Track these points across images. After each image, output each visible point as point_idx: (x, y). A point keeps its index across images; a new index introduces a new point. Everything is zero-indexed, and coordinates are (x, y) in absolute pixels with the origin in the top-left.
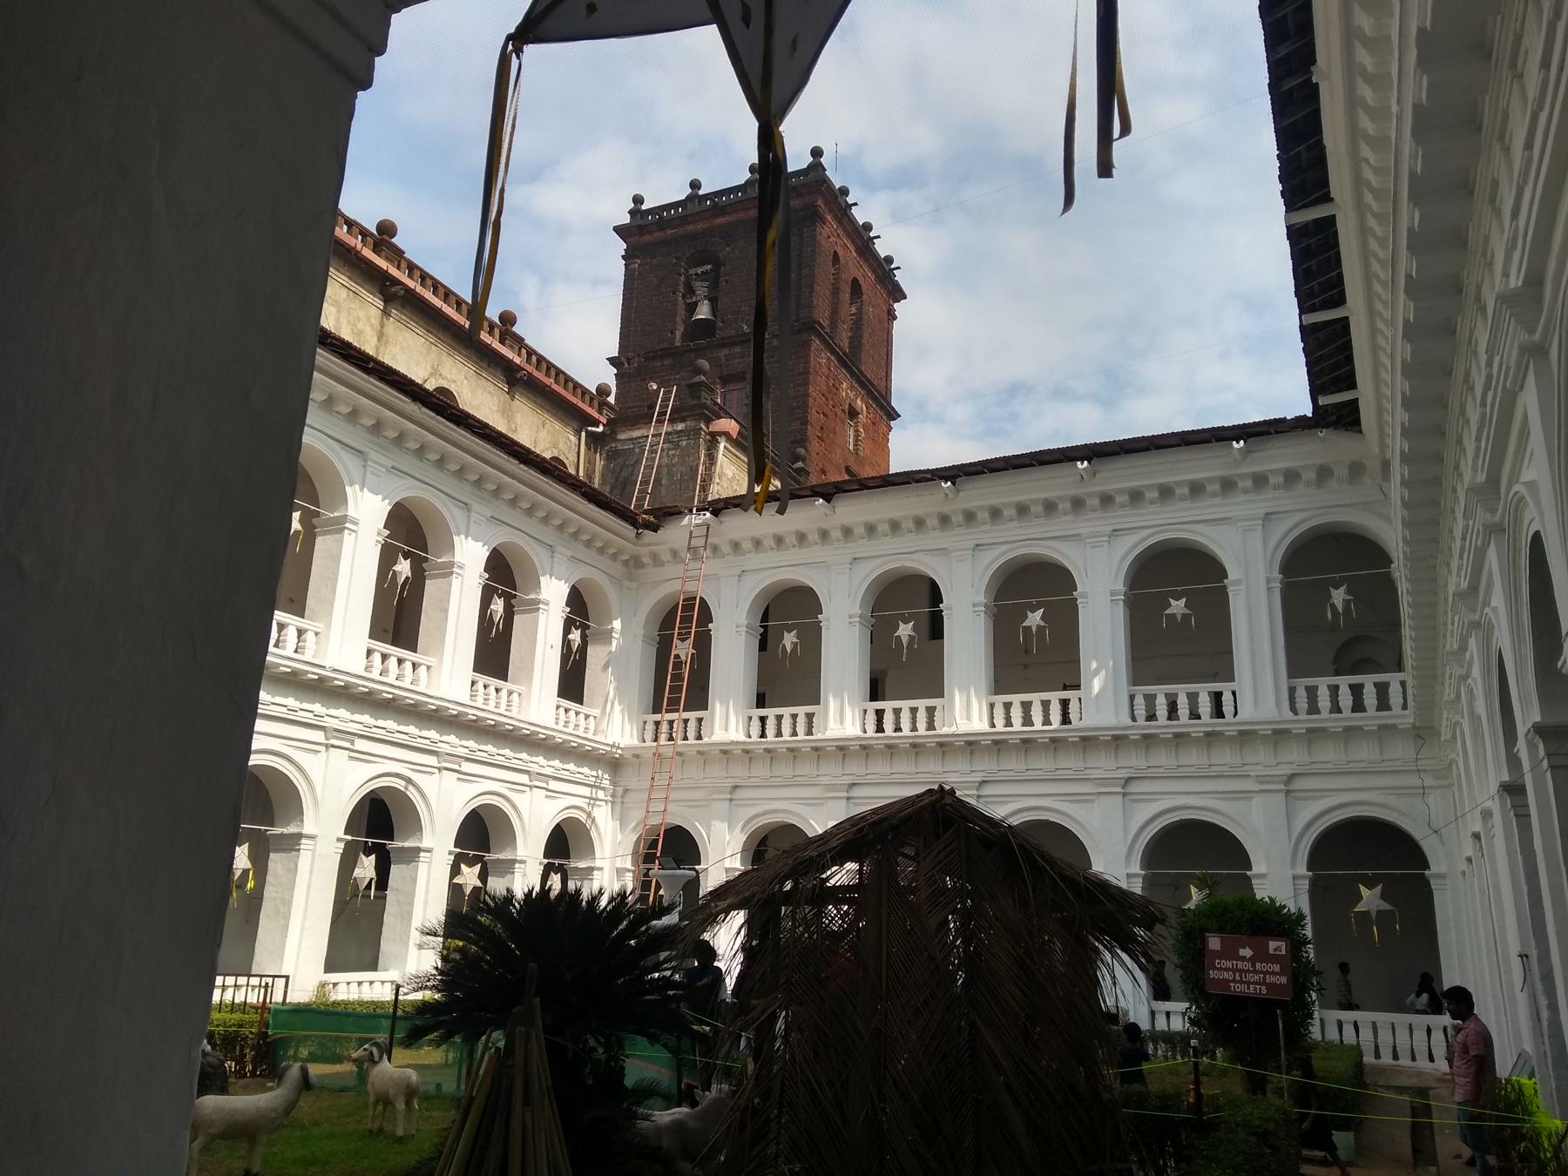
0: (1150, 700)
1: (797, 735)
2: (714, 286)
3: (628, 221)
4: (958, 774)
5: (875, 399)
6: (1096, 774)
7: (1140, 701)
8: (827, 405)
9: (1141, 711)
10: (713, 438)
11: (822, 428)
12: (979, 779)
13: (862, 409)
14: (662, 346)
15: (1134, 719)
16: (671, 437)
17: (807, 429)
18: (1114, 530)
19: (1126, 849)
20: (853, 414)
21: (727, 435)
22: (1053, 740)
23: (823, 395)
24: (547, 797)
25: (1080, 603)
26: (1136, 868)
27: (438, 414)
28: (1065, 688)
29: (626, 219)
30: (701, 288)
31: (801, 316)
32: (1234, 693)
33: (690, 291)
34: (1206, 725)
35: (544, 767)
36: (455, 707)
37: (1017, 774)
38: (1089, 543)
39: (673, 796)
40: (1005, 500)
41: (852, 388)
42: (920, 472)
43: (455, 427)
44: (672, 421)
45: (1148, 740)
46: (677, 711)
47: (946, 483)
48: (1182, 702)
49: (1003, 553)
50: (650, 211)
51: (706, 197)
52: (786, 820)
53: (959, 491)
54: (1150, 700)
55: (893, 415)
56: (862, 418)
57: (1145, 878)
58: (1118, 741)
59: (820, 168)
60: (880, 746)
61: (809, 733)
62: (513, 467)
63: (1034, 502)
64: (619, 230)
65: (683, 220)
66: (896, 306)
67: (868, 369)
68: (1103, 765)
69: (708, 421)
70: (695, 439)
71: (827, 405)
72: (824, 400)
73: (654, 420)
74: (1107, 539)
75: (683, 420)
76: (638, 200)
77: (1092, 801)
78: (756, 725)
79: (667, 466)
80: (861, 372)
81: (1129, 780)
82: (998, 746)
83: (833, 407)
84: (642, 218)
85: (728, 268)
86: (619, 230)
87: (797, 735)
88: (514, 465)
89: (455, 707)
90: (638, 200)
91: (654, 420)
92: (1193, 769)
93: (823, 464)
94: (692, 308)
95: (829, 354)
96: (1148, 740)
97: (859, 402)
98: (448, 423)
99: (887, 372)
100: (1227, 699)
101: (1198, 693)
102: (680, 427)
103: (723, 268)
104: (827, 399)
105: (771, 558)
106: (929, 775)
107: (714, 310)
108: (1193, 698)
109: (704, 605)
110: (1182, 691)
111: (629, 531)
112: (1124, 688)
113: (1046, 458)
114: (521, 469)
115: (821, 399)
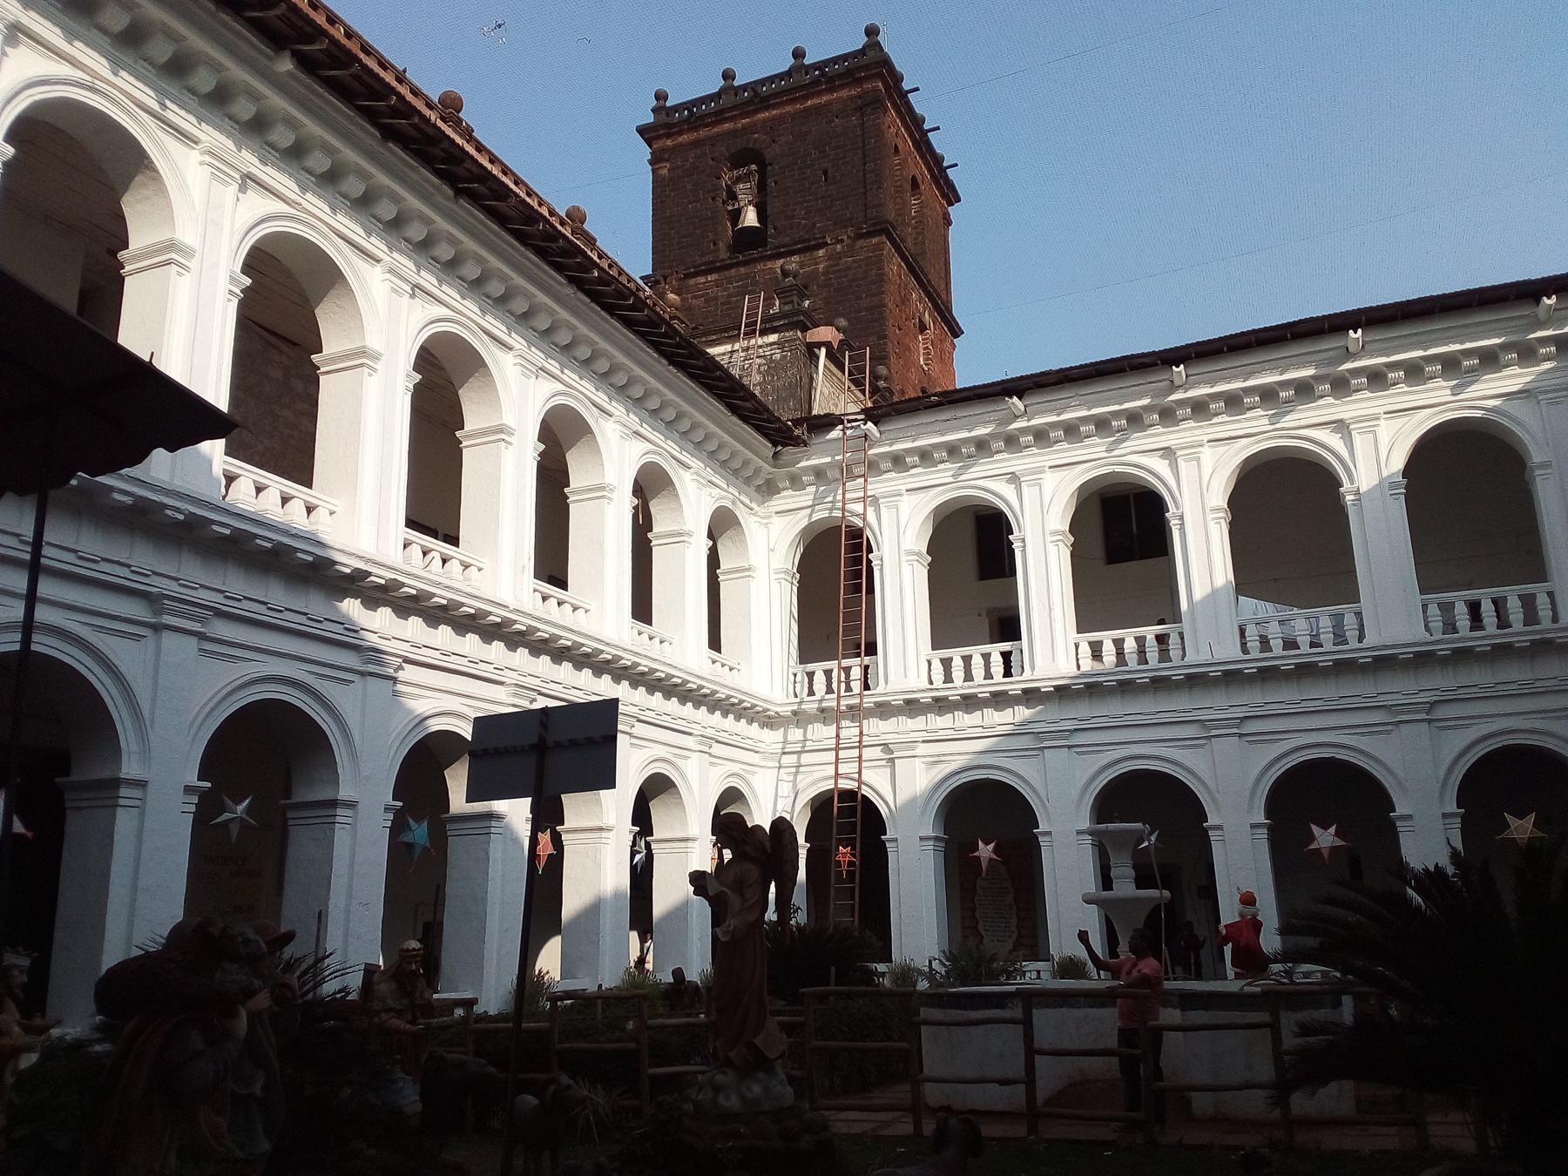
0: (1447, 608)
1: (814, 695)
2: (762, 187)
3: (652, 120)
4: (1211, 711)
6: (1390, 700)
7: (1433, 610)
9: (1436, 624)
12: (1242, 715)
14: (706, 259)
15: (1245, 650)
16: (761, 350)
17: (885, 344)
19: (1440, 785)
20: (923, 328)
21: (828, 345)
22: (1154, 680)
24: (711, 764)
26: (1452, 807)
27: (593, 301)
28: (1161, 622)
29: (650, 118)
30: (744, 191)
31: (869, 216)
32: (1551, 595)
33: (733, 196)
34: (1493, 637)
35: (706, 728)
36: (631, 657)
37: (1325, 703)
39: (867, 753)
42: (1143, 355)
43: (609, 318)
44: (763, 333)
45: (1462, 656)
46: (858, 655)
47: (1178, 367)
48: (1487, 608)
49: (1247, 447)
50: (676, 108)
51: (744, 88)
52: (990, 777)
54: (1447, 608)
57: (1463, 817)
58: (1422, 660)
59: (877, 48)
60: (1145, 680)
61: (1008, 673)
62: (663, 369)
64: (642, 131)
65: (719, 116)
66: (950, 209)
68: (1216, 705)
69: (805, 329)
70: (791, 351)
73: (742, 331)
75: (774, 330)
76: (661, 96)
77: (1388, 732)
78: (938, 668)
79: (760, 384)
80: (929, 281)
81: (1433, 704)
82: (1091, 690)
84: (668, 115)
85: (777, 167)
86: (642, 131)
87: (814, 695)
88: (663, 366)
89: (631, 657)
90: (661, 96)
91: (742, 331)
92: (1515, 686)
93: (903, 385)
94: (736, 215)
95: (899, 260)
96: (1462, 656)
98: (603, 313)
99: (946, 285)
100: (1542, 601)
101: (1535, 594)
102: (773, 338)
103: (769, 168)
105: (944, 473)
106: (1139, 717)
107: (761, 216)
108: (1499, 604)
109: (856, 534)
110: (1485, 596)
111: (767, 448)
112: (1417, 598)
114: (669, 371)
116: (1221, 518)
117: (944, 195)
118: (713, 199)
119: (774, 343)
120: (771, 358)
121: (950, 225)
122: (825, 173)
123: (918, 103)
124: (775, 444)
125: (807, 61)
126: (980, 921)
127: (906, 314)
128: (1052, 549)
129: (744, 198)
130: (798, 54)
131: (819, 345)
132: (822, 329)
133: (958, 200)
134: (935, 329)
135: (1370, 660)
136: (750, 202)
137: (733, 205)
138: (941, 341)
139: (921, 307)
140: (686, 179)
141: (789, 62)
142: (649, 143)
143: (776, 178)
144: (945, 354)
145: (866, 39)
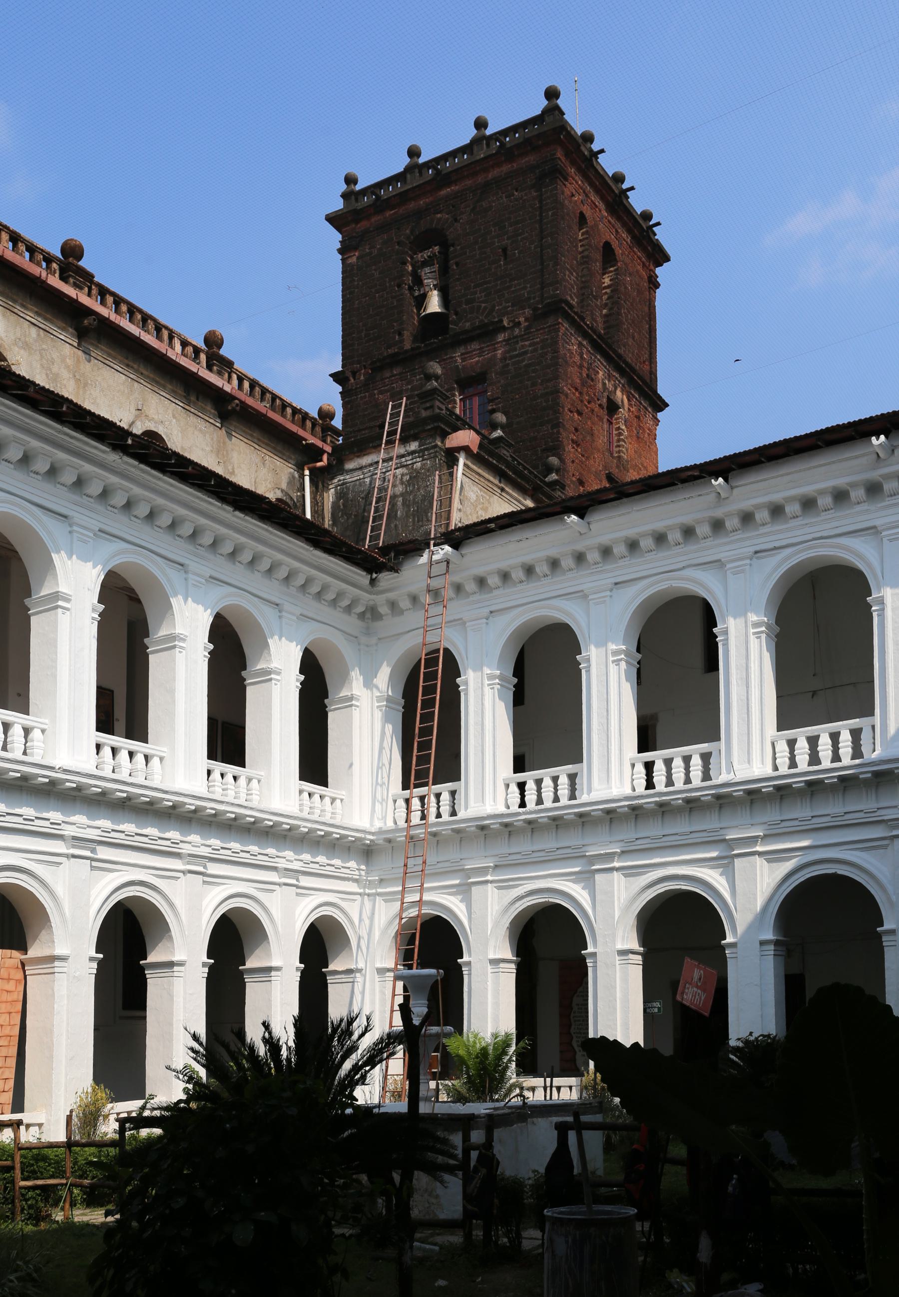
5: (638, 388)
8: (582, 401)
10: (451, 458)
11: (576, 430)
13: (622, 401)
16: (403, 460)
17: (558, 433)
18: (756, 552)
21: (466, 449)
23: (576, 389)
25: (721, 641)
38: (591, 600)
40: (670, 522)
41: (610, 377)
44: (404, 440)
47: (716, 480)
53: (732, 488)
55: (659, 405)
56: (623, 412)
63: (670, 528)
66: (658, 271)
67: (630, 353)
69: (444, 435)
71: (582, 401)
72: (577, 394)
73: (384, 441)
74: (485, 620)
75: (415, 438)
79: (402, 495)
80: (620, 356)
83: (589, 402)
91: (384, 441)
97: (619, 393)
102: (414, 446)
104: (581, 393)
113: (747, 459)
115: (574, 394)
116: (762, 632)
117: (650, 256)
118: (399, 286)
119: (413, 453)
120: (413, 467)
121: (658, 287)
122: (505, 250)
123: (608, 164)
124: (369, 571)
125: (489, 132)
126: (574, 1036)
127: (589, 395)
128: (487, 689)
129: (429, 282)
130: (481, 124)
131: (459, 449)
132: (460, 433)
133: (667, 259)
134: (630, 405)
135: (869, 775)
136: (435, 287)
137: (419, 290)
138: (638, 417)
139: (610, 385)
140: (374, 267)
141: (473, 132)
142: (338, 228)
143: (457, 260)
144: (644, 431)
145: (546, 102)
